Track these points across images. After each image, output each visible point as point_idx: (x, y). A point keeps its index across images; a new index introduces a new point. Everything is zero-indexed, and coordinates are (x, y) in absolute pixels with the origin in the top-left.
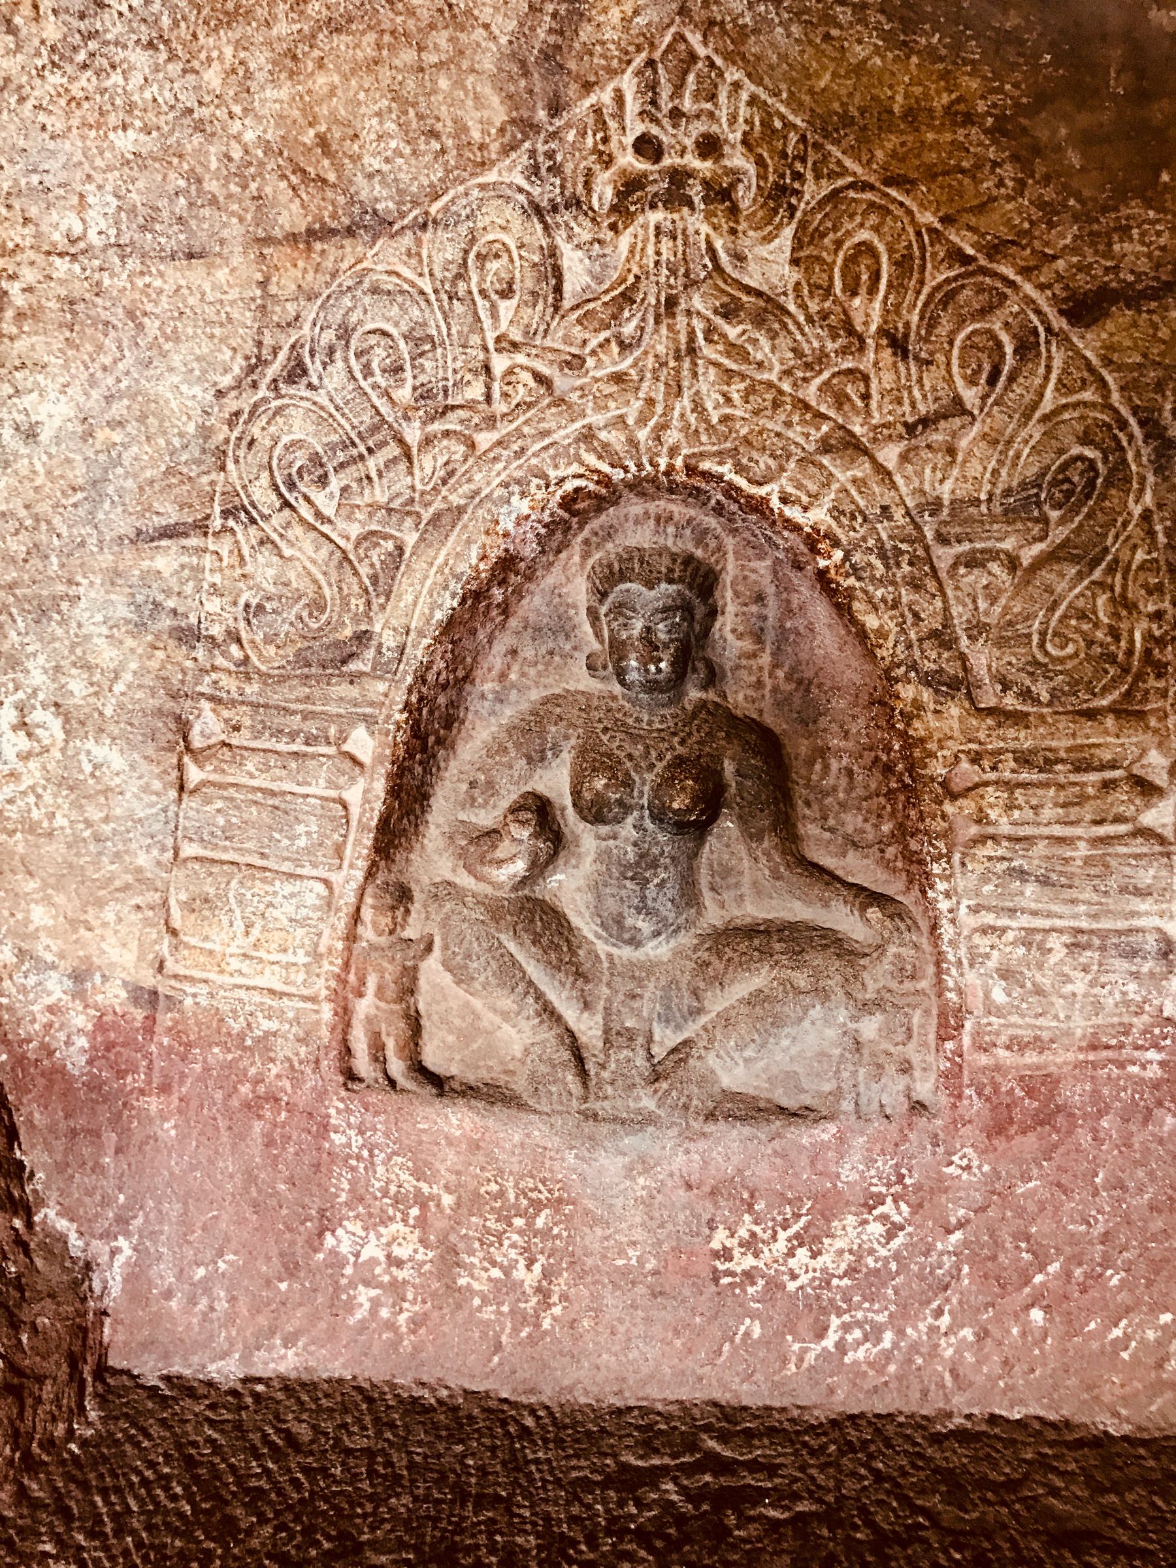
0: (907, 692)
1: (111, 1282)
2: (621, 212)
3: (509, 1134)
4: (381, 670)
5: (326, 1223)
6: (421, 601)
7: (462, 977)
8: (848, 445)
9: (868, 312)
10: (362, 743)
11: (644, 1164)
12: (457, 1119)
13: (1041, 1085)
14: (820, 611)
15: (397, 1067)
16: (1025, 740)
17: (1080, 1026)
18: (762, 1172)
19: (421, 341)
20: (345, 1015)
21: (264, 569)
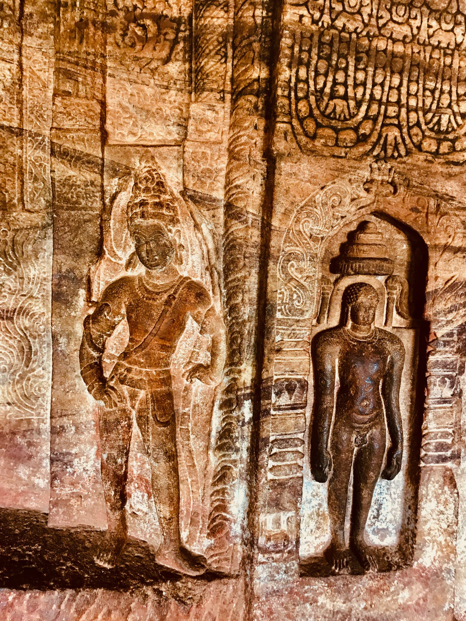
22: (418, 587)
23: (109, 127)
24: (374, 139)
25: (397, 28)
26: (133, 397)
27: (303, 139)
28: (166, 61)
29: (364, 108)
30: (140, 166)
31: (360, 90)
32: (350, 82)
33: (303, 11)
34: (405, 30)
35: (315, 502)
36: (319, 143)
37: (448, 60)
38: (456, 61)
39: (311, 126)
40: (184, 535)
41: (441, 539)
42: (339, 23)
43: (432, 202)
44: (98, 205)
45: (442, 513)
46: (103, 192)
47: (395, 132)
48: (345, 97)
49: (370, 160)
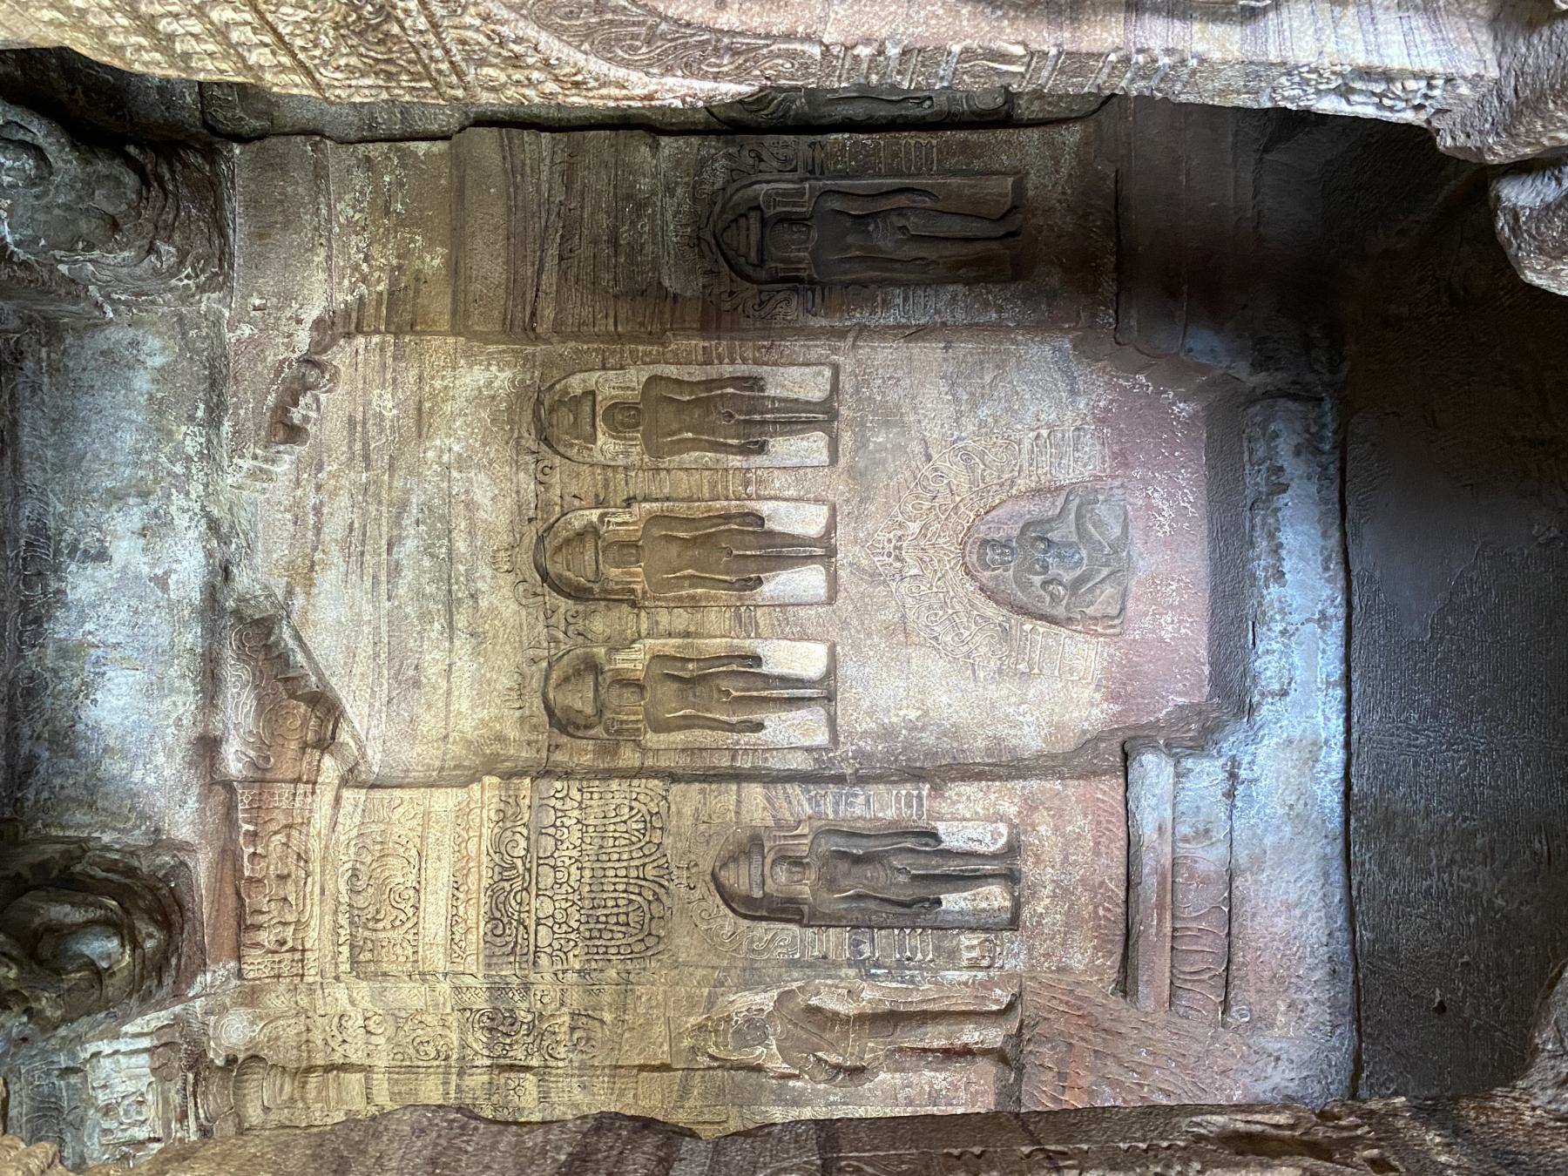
0: (1014, 492)
1: (1181, 700)
2: (902, 560)
3: (1134, 589)
4: (1008, 621)
5: (1162, 640)
6: (990, 609)
7: (1092, 603)
8: (956, 507)
9: (927, 505)
10: (1028, 627)
11: (1140, 554)
12: (1131, 605)
13: (1114, 456)
14: (993, 513)
15: (1117, 622)
16: (1026, 465)
17: (1098, 448)
18: (1141, 525)
19: (930, 608)
20: (1102, 635)
21: (983, 650)
22: (1036, 817)
23: (657, 1062)
24: (657, 889)
25: (573, 878)
26: (872, 1050)
27: (661, 947)
28: (602, 1021)
29: (633, 897)
30: (687, 1043)
31: (621, 902)
32: (615, 910)
33: (571, 955)
34: (573, 869)
35: (963, 904)
36: (662, 933)
37: (591, 829)
38: (590, 822)
39: (651, 941)
40: (995, 1008)
41: (993, 797)
42: (575, 925)
43: (702, 827)
44: (720, 1072)
45: (969, 798)
46: (710, 1068)
47: (649, 867)
48: (627, 914)
49: (672, 886)
